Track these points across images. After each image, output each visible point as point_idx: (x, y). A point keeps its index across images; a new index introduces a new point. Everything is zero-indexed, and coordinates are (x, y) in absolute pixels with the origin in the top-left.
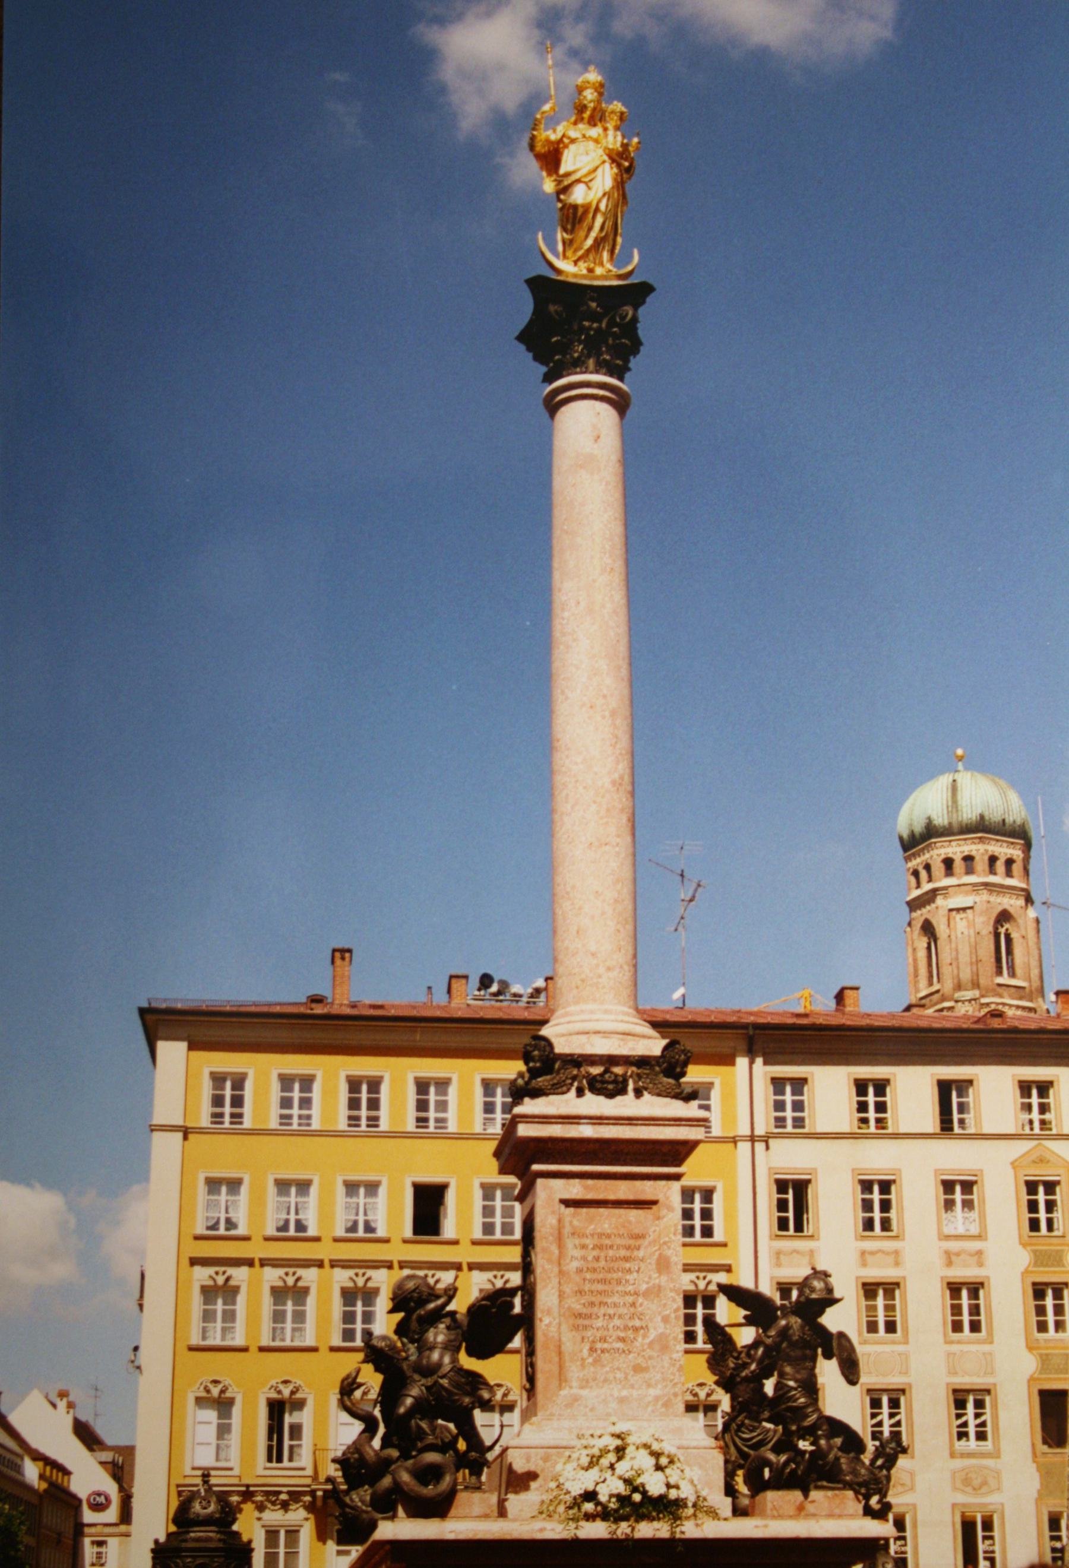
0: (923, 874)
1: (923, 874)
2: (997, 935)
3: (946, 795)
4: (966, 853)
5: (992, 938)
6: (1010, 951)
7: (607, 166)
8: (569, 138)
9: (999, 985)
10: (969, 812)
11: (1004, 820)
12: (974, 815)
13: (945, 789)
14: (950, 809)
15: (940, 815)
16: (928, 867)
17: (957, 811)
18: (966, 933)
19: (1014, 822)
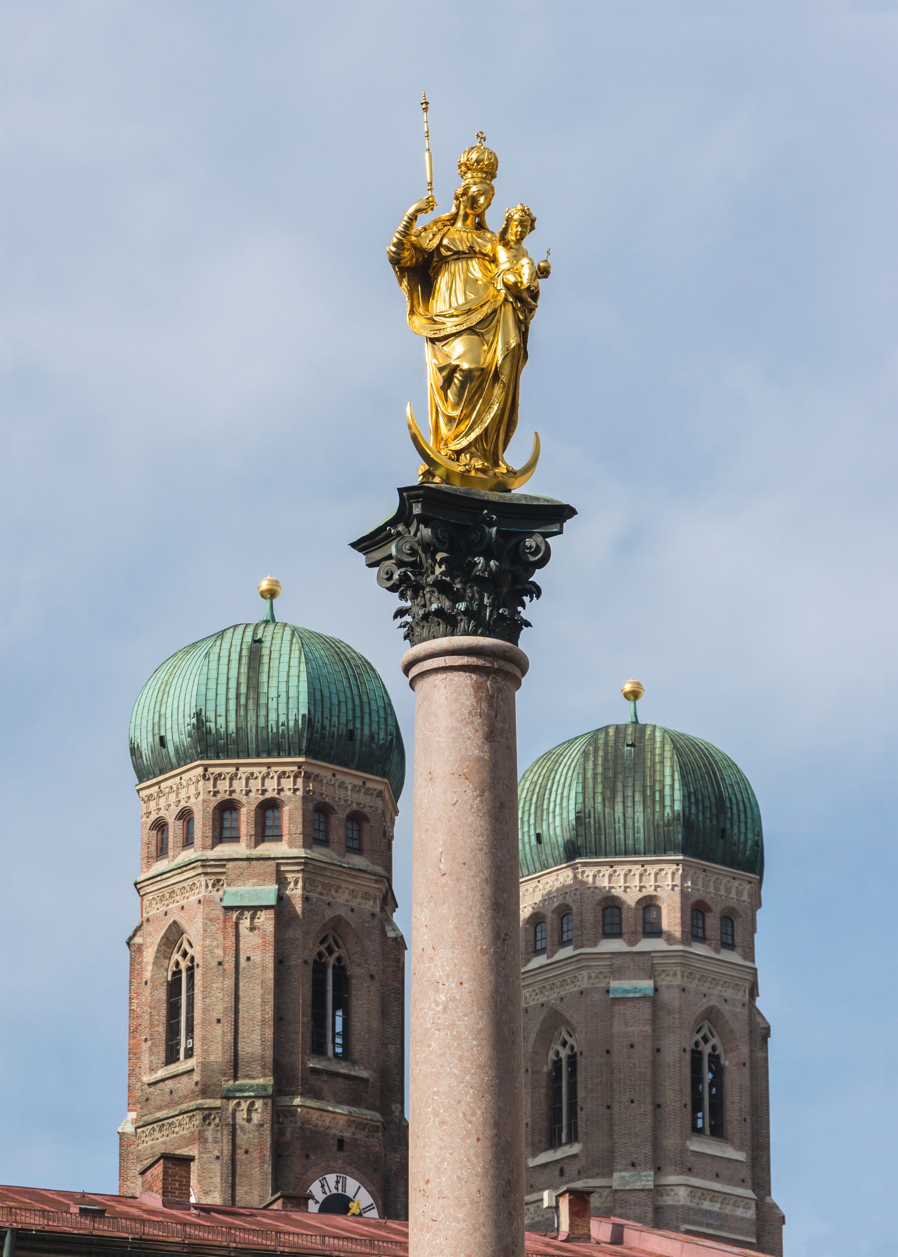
0: (175, 829)
1: (175, 829)
2: (319, 968)
3: (236, 671)
4: (268, 795)
5: (308, 972)
6: (342, 1002)
7: (509, 308)
8: (448, 249)
9: (314, 1071)
10: (282, 710)
11: (351, 734)
12: (292, 717)
13: (235, 657)
14: (243, 701)
15: (221, 710)
16: (186, 815)
17: (258, 705)
18: (256, 957)
19: (372, 736)
